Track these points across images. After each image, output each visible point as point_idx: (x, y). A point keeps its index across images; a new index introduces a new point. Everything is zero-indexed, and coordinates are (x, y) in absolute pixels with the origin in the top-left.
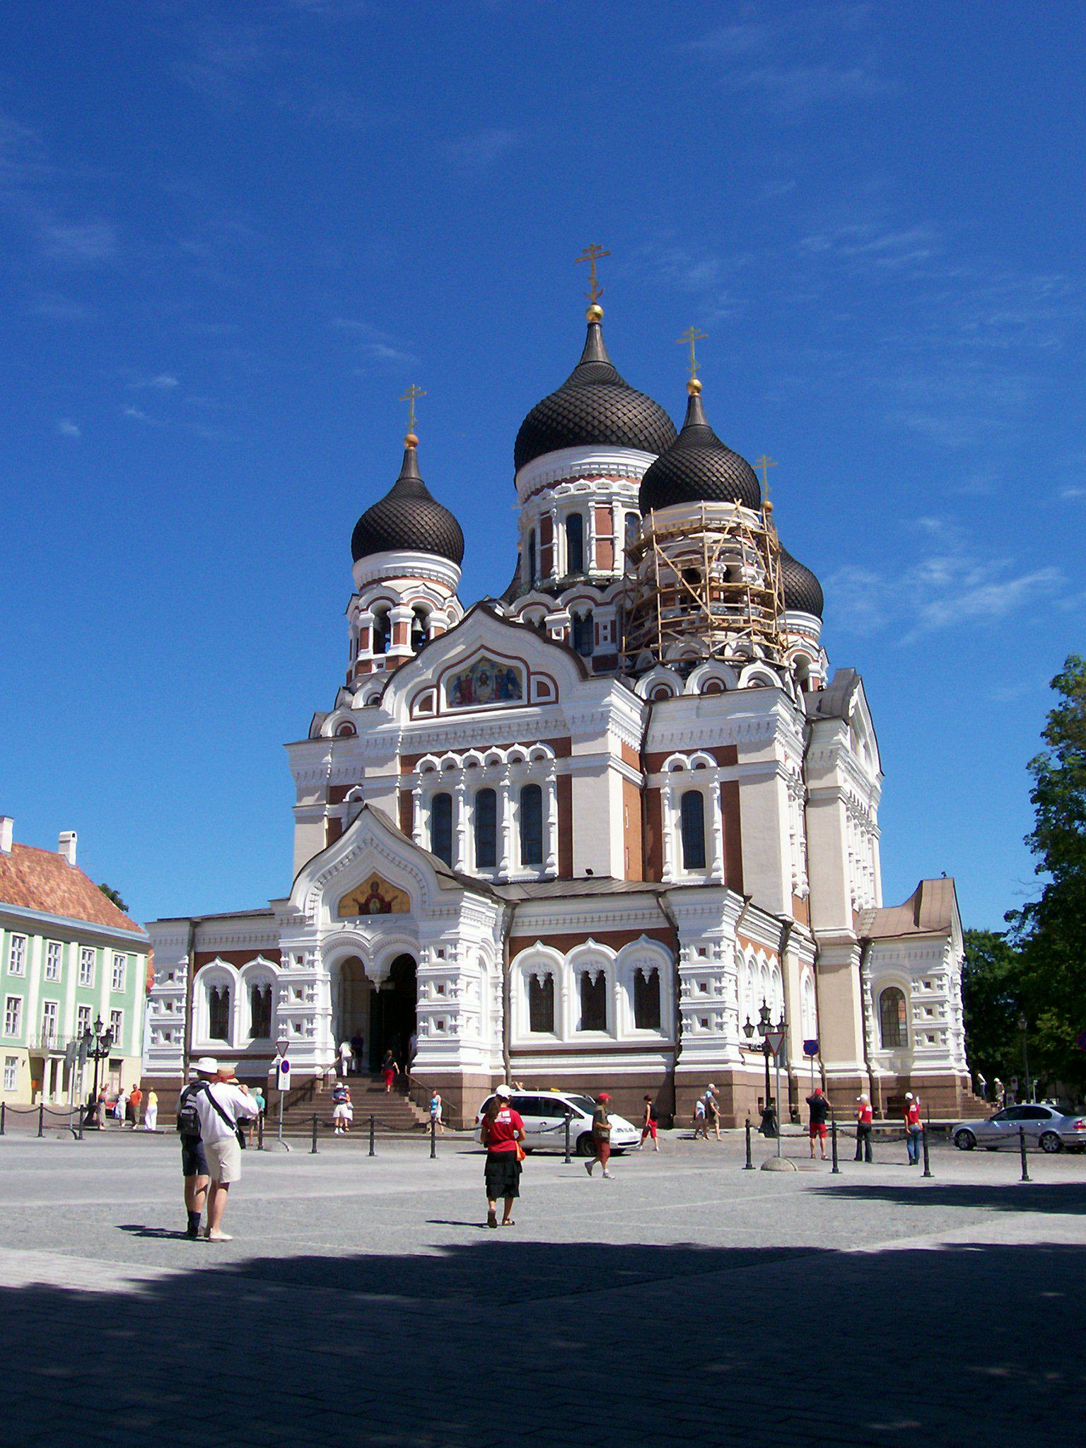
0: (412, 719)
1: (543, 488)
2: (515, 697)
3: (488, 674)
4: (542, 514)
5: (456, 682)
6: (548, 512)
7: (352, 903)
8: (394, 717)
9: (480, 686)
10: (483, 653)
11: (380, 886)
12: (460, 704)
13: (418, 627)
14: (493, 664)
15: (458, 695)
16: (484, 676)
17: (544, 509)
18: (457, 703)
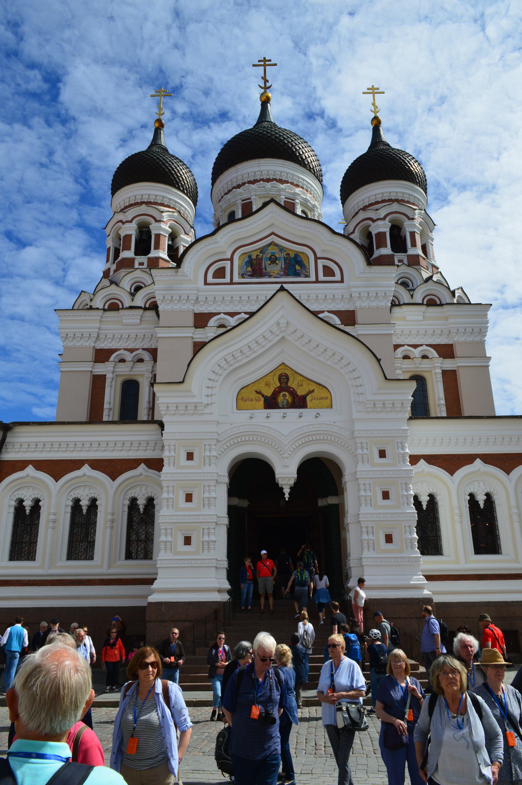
0: (206, 283)
1: (244, 184)
2: (302, 275)
3: (277, 255)
4: (243, 201)
5: (247, 259)
6: (250, 199)
7: (254, 395)
8: (192, 278)
9: (270, 264)
10: (273, 238)
11: (291, 379)
12: (252, 276)
13: (170, 243)
14: (282, 249)
15: (249, 269)
16: (273, 257)
17: (245, 196)
18: (249, 275)
